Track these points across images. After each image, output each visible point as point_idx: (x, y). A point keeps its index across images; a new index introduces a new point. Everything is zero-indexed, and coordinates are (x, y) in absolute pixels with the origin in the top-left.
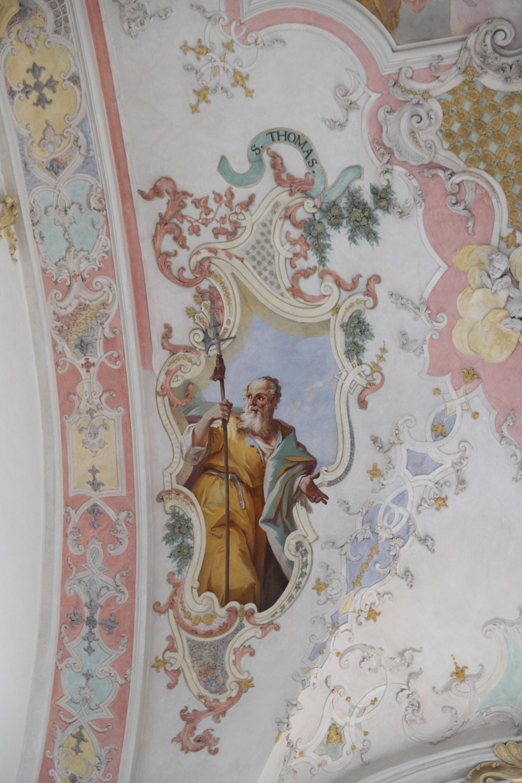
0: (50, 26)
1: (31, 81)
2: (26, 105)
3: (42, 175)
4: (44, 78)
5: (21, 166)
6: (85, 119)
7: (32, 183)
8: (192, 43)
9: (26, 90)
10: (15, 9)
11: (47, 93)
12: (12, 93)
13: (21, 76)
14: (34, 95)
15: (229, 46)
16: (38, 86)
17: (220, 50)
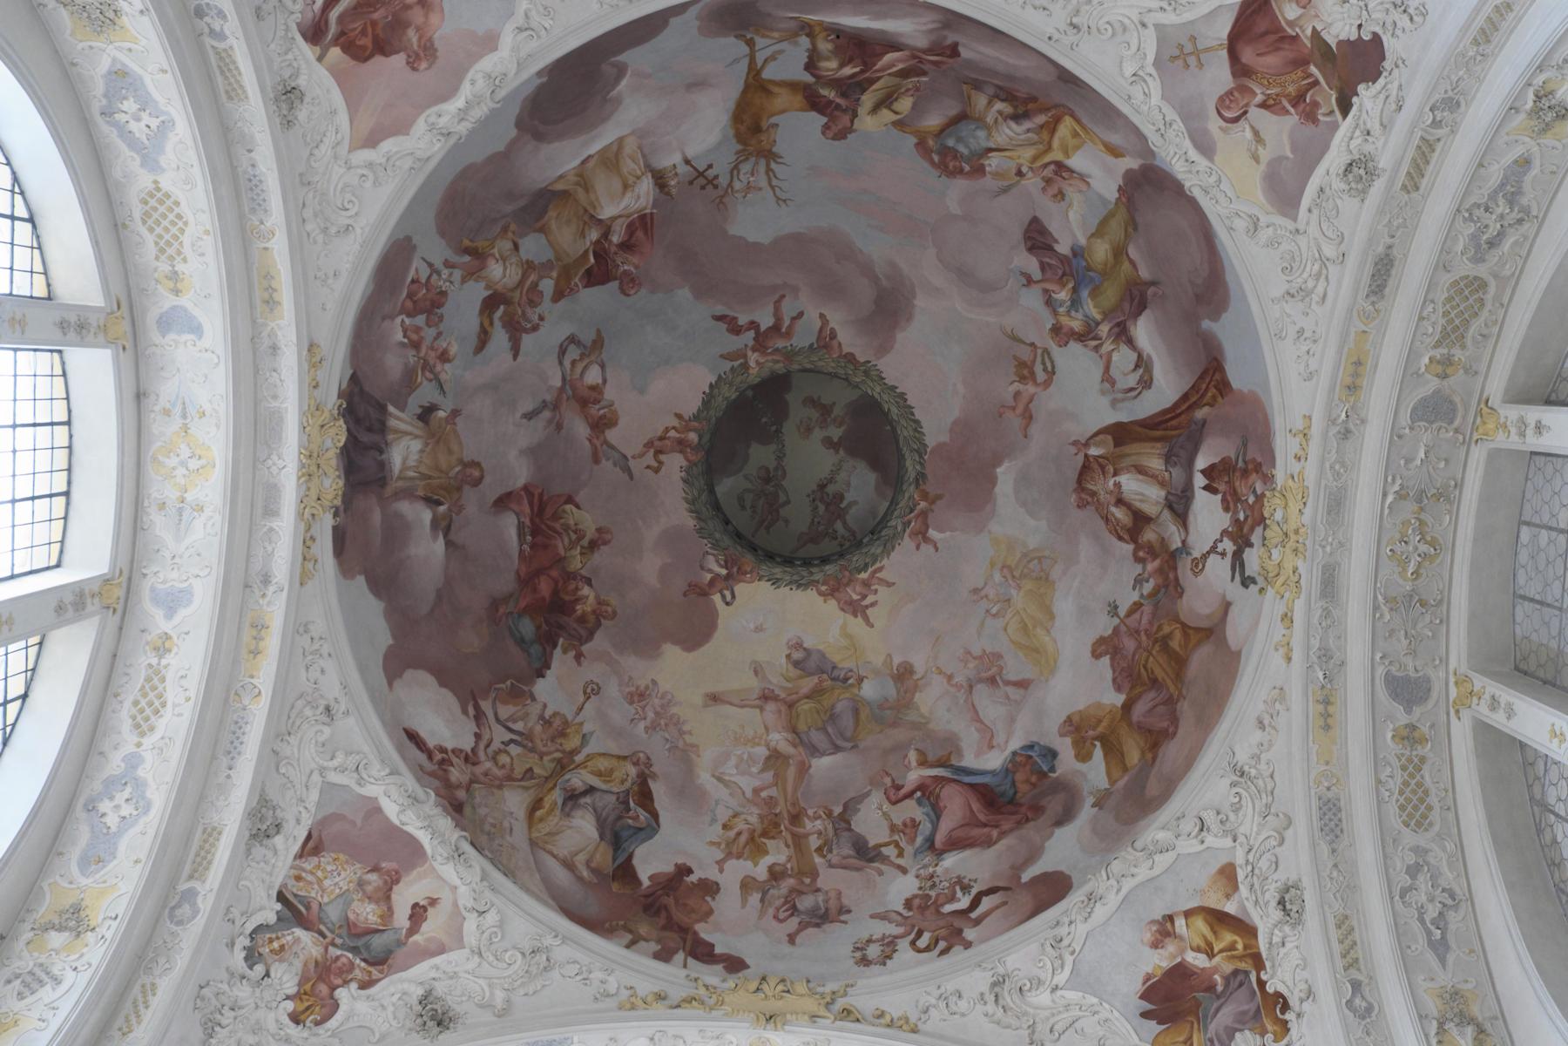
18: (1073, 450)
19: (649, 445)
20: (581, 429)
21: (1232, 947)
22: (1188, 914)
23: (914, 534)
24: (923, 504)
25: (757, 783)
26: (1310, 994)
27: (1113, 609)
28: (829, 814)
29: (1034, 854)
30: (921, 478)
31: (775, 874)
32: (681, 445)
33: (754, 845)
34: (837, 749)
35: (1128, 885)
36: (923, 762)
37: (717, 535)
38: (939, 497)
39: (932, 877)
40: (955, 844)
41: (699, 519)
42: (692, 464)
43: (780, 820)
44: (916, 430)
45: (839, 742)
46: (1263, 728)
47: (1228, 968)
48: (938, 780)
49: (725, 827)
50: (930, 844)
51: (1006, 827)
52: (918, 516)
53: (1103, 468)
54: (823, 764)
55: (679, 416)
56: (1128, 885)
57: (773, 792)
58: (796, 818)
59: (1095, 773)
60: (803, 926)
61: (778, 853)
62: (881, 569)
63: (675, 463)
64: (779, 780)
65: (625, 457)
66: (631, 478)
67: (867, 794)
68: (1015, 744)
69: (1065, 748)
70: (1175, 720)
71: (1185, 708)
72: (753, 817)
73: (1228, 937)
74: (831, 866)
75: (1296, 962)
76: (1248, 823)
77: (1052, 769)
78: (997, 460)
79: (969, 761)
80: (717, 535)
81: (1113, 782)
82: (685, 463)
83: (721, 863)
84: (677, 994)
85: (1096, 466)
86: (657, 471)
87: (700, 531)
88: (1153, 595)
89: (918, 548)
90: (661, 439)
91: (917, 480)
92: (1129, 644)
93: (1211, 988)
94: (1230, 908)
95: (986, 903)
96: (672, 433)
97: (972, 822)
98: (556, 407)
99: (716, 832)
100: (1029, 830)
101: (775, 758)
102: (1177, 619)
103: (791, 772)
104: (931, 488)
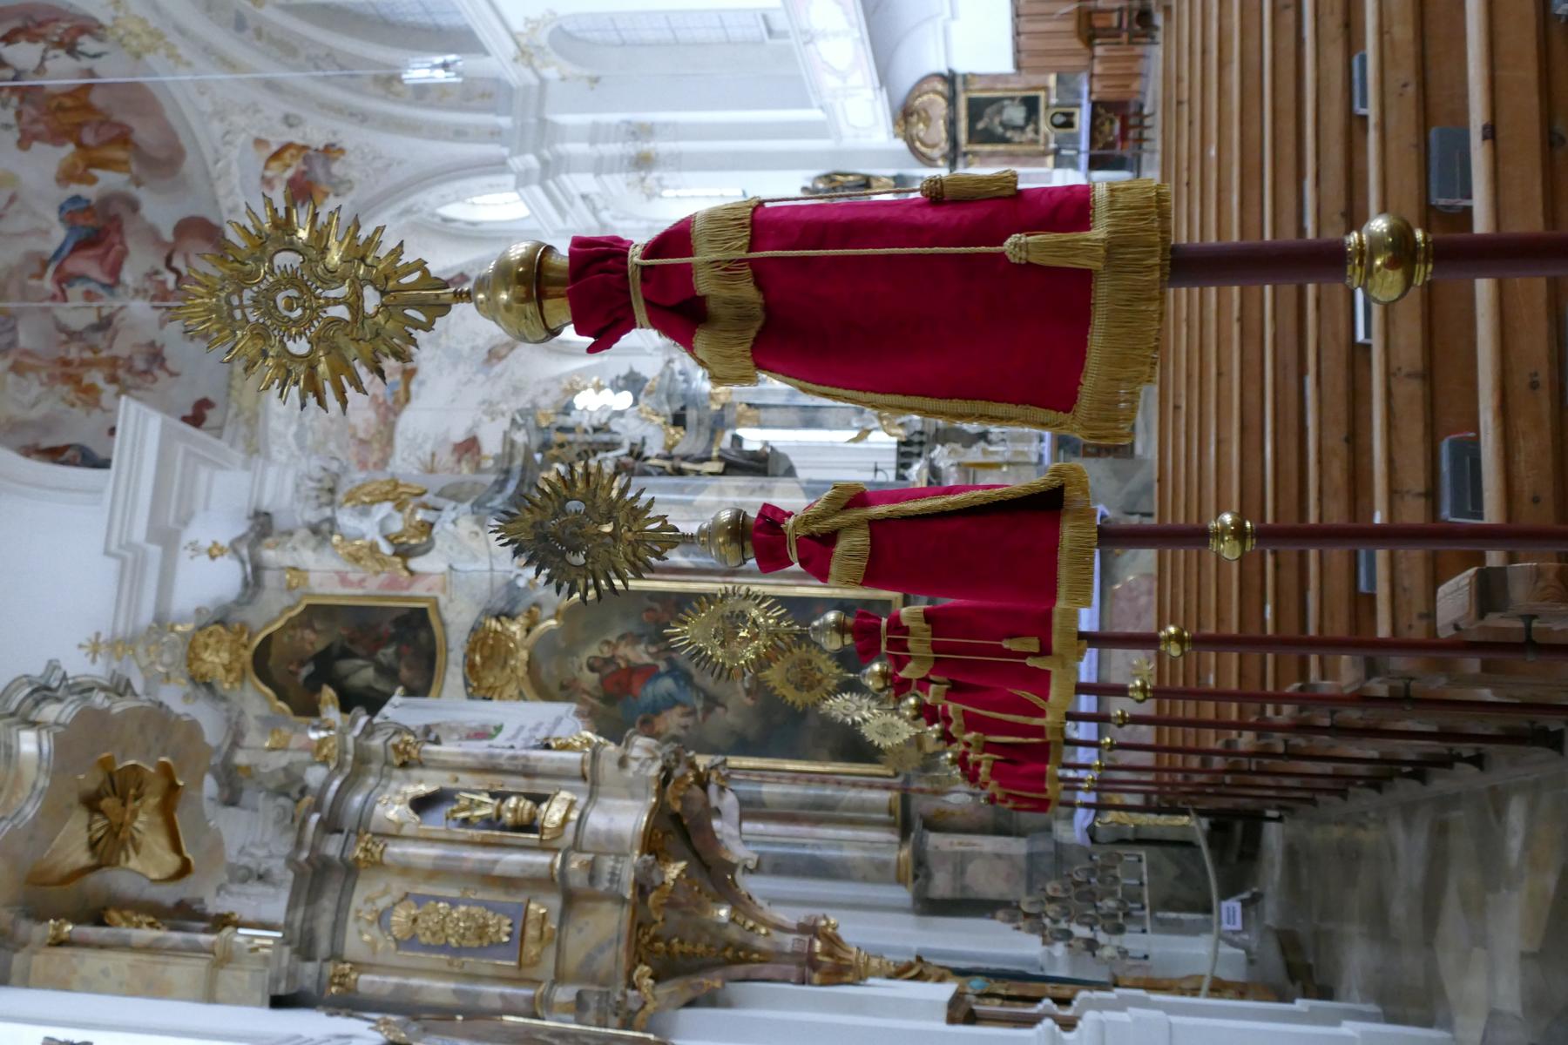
21: (292, 156)
22: (266, 167)
25: (36, 383)
26: (335, 133)
27: (7, 127)
28: (65, 343)
29: (153, 234)
31: (113, 379)
33: (91, 390)
34: (14, 329)
35: (238, 190)
36: (40, 276)
39: (137, 291)
40: (115, 271)
43: (68, 374)
45: (9, 326)
46: (202, 94)
47: (300, 161)
48: (58, 270)
49: (73, 405)
50: (104, 286)
51: (116, 239)
54: (25, 340)
56: (238, 190)
57: (44, 375)
58: (66, 363)
59: (109, 181)
60: (162, 366)
61: (96, 377)
64: (32, 368)
67: (55, 317)
68: (53, 216)
69: (75, 189)
70: (120, 125)
71: (118, 117)
72: (64, 389)
73: (287, 155)
74: (110, 346)
75: (315, 133)
76: (240, 120)
77: (88, 201)
79: (50, 248)
81: (129, 171)
83: (104, 411)
84: (243, 430)
88: (22, 100)
92: (40, 127)
93: (304, 173)
94: (275, 148)
95: (178, 262)
97: (101, 260)
99: (78, 412)
100: (129, 227)
101: (17, 368)
102: (54, 96)
103: (29, 361)
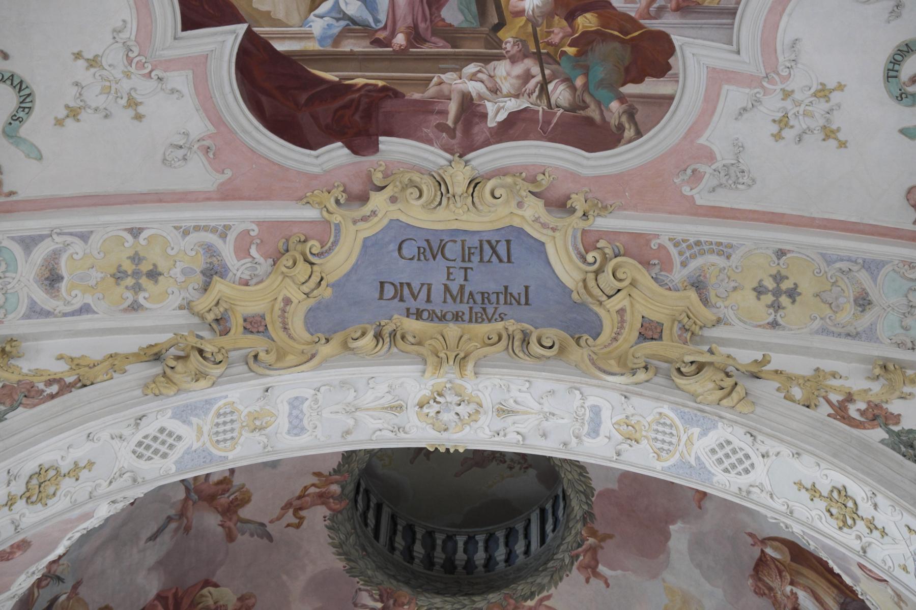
0: (720, 261)
1: (769, 298)
2: (791, 312)
3: (867, 318)
4: (770, 284)
5: (849, 341)
6: (823, 256)
7: (870, 335)
8: (775, 128)
9: (776, 307)
10: (693, 295)
11: (785, 286)
12: (774, 325)
13: (760, 309)
14: (784, 300)
15: (787, 94)
16: (777, 293)
17: (788, 104)
18: (750, 541)
19: (286, 507)
20: (211, 521)
23: (583, 568)
24: (591, 540)
30: (588, 517)
32: (323, 498)
37: (370, 573)
38: (610, 537)
41: (348, 560)
42: (336, 513)
44: (581, 474)
52: (586, 551)
53: (780, 572)
55: (318, 474)
62: (548, 597)
63: (317, 516)
65: (263, 525)
66: (270, 538)
78: (671, 518)
80: (370, 573)
82: (328, 513)
85: (773, 566)
86: (298, 526)
87: (350, 571)
89: (587, 581)
90: (299, 498)
91: (584, 519)
96: (312, 490)
98: (182, 514)
104: (600, 527)
